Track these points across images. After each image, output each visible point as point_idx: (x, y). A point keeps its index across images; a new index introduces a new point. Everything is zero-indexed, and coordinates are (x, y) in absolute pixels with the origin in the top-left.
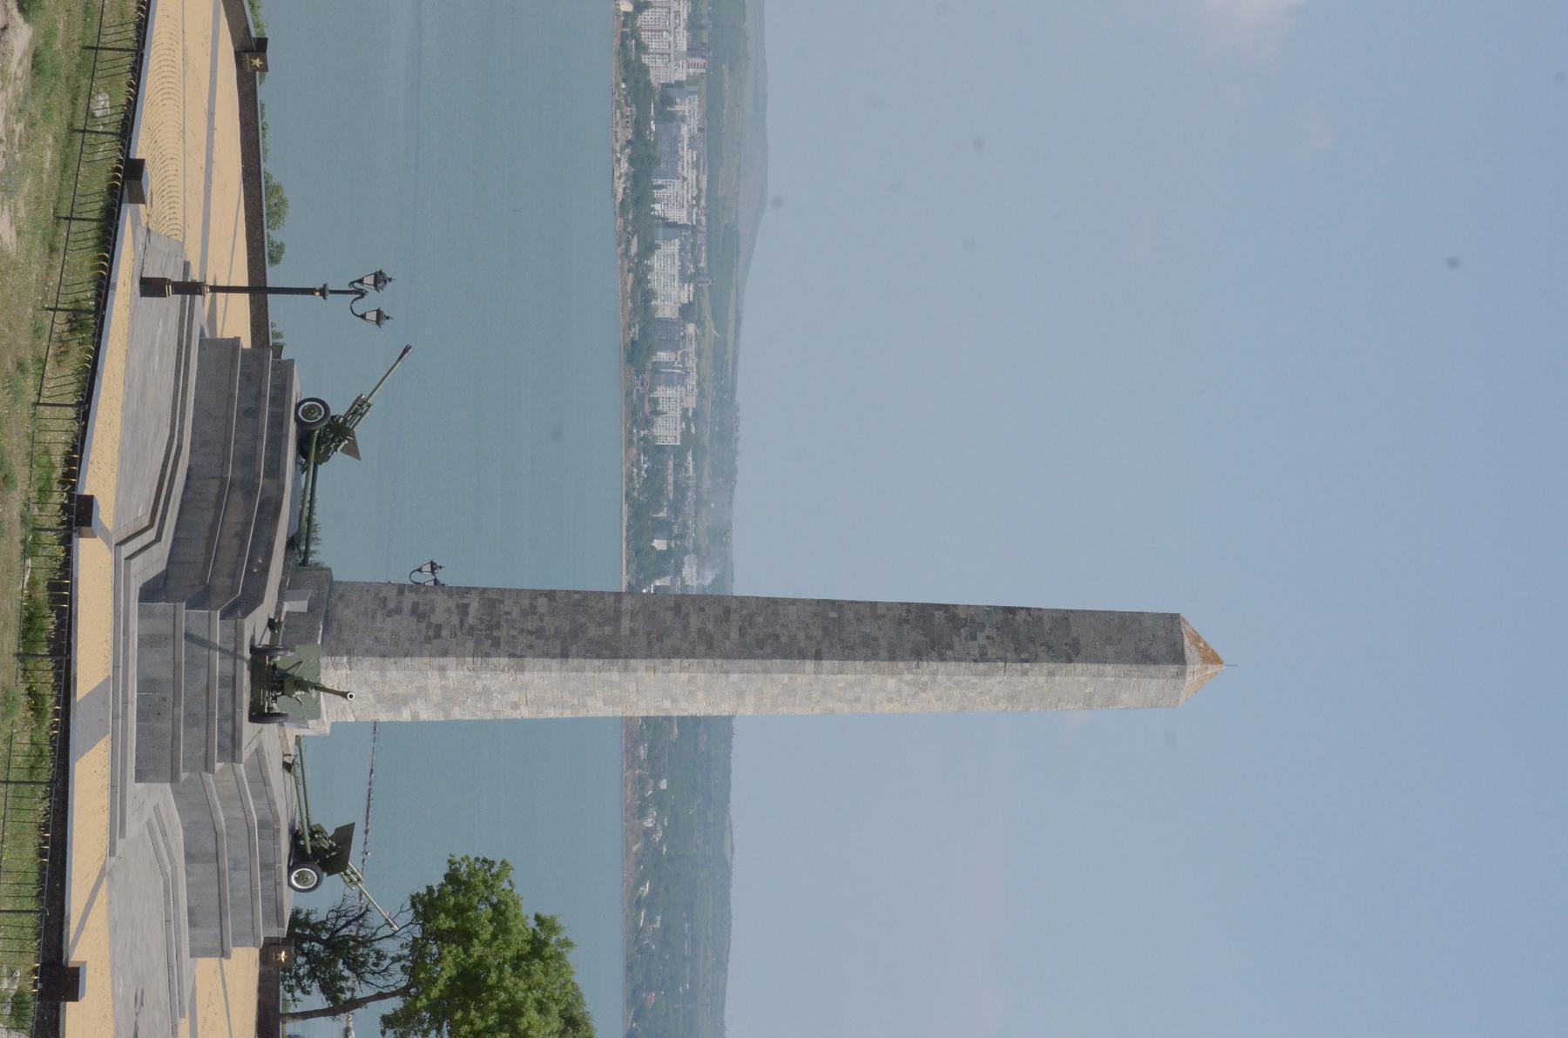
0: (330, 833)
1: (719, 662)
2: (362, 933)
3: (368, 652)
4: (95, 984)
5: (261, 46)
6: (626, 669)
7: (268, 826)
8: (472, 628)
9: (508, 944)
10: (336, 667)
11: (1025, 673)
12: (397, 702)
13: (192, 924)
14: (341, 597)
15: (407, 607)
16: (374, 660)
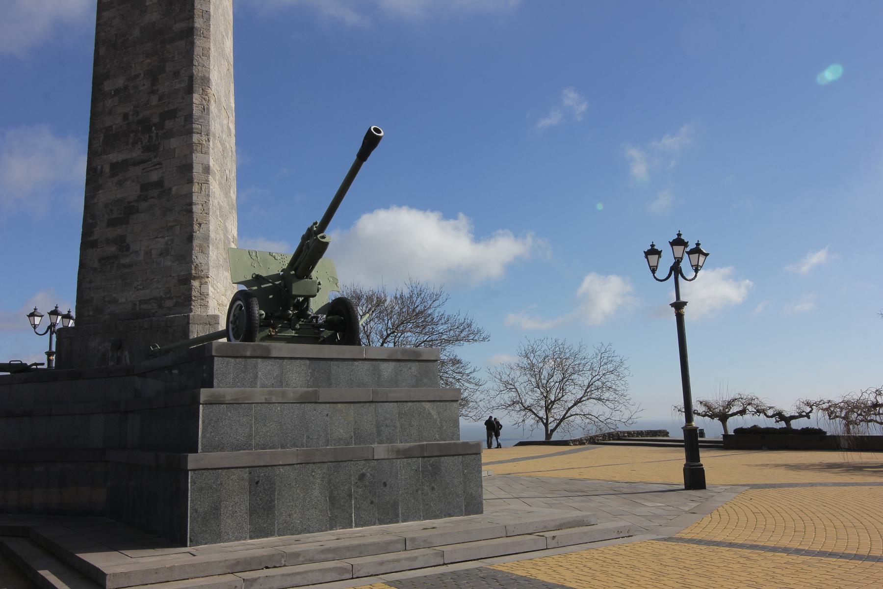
8: (147, 149)
15: (113, 233)
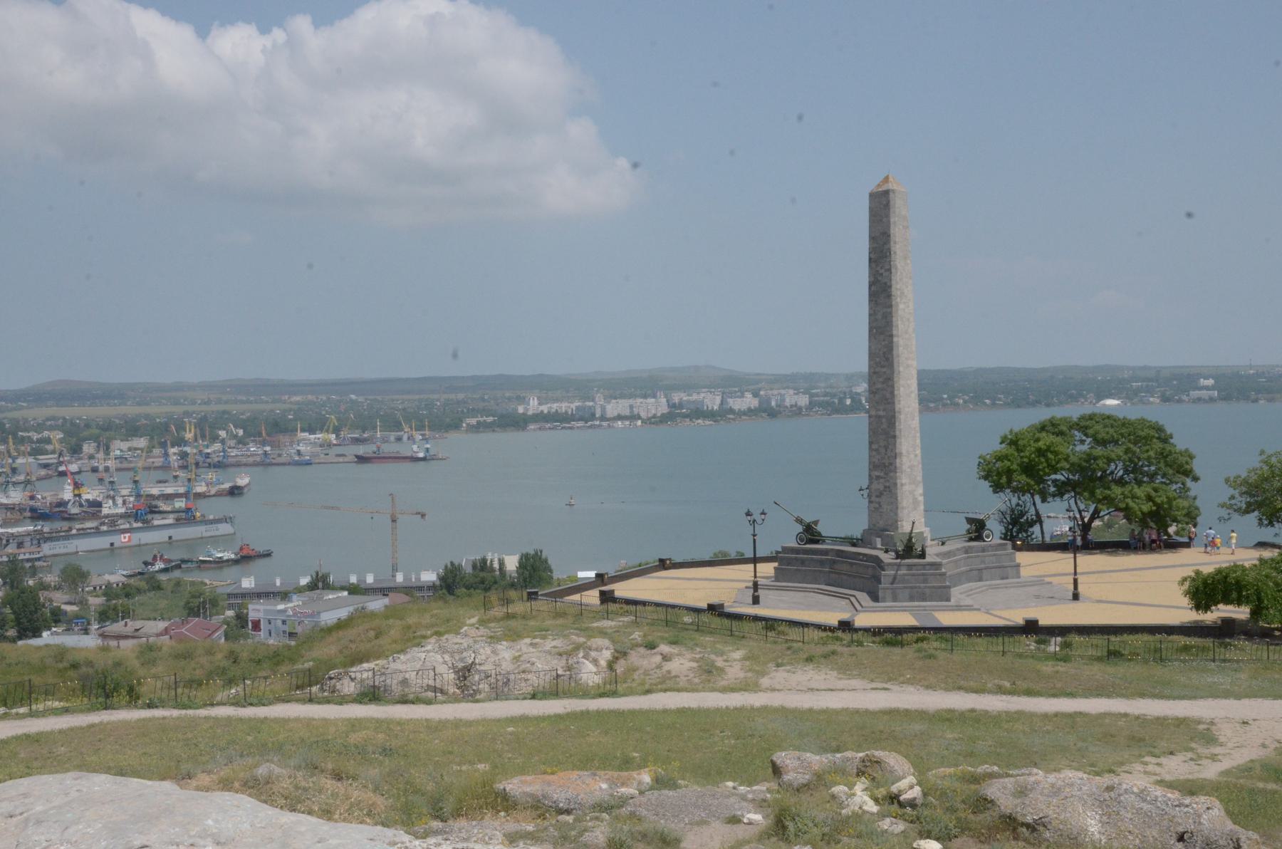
0: (969, 526)
1: (895, 375)
2: (1009, 512)
3: (896, 514)
4: (1031, 614)
5: (662, 561)
6: (900, 412)
7: (967, 551)
8: (886, 474)
9: (1012, 455)
10: (903, 526)
11: (895, 253)
12: (915, 501)
13: (1007, 578)
14: (874, 525)
15: (877, 500)
16: (899, 511)
